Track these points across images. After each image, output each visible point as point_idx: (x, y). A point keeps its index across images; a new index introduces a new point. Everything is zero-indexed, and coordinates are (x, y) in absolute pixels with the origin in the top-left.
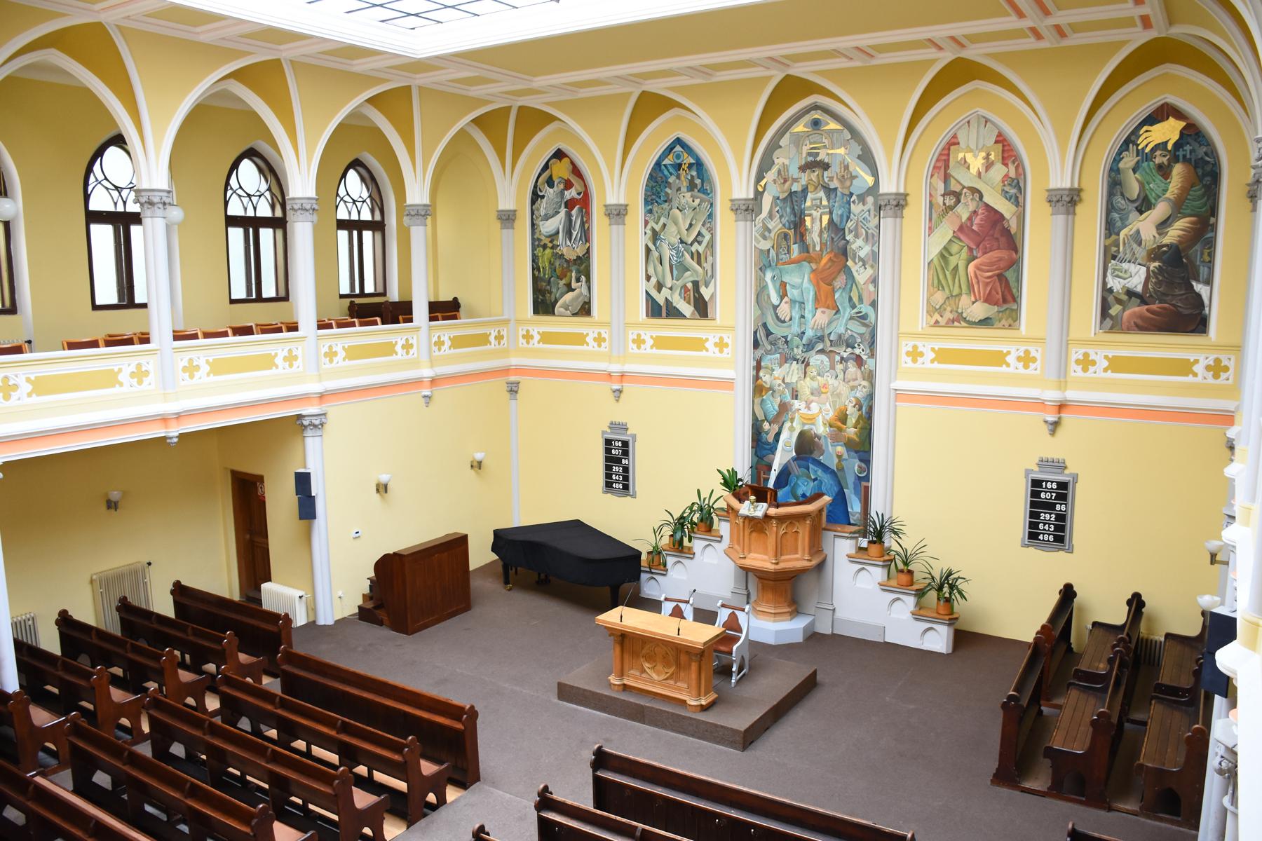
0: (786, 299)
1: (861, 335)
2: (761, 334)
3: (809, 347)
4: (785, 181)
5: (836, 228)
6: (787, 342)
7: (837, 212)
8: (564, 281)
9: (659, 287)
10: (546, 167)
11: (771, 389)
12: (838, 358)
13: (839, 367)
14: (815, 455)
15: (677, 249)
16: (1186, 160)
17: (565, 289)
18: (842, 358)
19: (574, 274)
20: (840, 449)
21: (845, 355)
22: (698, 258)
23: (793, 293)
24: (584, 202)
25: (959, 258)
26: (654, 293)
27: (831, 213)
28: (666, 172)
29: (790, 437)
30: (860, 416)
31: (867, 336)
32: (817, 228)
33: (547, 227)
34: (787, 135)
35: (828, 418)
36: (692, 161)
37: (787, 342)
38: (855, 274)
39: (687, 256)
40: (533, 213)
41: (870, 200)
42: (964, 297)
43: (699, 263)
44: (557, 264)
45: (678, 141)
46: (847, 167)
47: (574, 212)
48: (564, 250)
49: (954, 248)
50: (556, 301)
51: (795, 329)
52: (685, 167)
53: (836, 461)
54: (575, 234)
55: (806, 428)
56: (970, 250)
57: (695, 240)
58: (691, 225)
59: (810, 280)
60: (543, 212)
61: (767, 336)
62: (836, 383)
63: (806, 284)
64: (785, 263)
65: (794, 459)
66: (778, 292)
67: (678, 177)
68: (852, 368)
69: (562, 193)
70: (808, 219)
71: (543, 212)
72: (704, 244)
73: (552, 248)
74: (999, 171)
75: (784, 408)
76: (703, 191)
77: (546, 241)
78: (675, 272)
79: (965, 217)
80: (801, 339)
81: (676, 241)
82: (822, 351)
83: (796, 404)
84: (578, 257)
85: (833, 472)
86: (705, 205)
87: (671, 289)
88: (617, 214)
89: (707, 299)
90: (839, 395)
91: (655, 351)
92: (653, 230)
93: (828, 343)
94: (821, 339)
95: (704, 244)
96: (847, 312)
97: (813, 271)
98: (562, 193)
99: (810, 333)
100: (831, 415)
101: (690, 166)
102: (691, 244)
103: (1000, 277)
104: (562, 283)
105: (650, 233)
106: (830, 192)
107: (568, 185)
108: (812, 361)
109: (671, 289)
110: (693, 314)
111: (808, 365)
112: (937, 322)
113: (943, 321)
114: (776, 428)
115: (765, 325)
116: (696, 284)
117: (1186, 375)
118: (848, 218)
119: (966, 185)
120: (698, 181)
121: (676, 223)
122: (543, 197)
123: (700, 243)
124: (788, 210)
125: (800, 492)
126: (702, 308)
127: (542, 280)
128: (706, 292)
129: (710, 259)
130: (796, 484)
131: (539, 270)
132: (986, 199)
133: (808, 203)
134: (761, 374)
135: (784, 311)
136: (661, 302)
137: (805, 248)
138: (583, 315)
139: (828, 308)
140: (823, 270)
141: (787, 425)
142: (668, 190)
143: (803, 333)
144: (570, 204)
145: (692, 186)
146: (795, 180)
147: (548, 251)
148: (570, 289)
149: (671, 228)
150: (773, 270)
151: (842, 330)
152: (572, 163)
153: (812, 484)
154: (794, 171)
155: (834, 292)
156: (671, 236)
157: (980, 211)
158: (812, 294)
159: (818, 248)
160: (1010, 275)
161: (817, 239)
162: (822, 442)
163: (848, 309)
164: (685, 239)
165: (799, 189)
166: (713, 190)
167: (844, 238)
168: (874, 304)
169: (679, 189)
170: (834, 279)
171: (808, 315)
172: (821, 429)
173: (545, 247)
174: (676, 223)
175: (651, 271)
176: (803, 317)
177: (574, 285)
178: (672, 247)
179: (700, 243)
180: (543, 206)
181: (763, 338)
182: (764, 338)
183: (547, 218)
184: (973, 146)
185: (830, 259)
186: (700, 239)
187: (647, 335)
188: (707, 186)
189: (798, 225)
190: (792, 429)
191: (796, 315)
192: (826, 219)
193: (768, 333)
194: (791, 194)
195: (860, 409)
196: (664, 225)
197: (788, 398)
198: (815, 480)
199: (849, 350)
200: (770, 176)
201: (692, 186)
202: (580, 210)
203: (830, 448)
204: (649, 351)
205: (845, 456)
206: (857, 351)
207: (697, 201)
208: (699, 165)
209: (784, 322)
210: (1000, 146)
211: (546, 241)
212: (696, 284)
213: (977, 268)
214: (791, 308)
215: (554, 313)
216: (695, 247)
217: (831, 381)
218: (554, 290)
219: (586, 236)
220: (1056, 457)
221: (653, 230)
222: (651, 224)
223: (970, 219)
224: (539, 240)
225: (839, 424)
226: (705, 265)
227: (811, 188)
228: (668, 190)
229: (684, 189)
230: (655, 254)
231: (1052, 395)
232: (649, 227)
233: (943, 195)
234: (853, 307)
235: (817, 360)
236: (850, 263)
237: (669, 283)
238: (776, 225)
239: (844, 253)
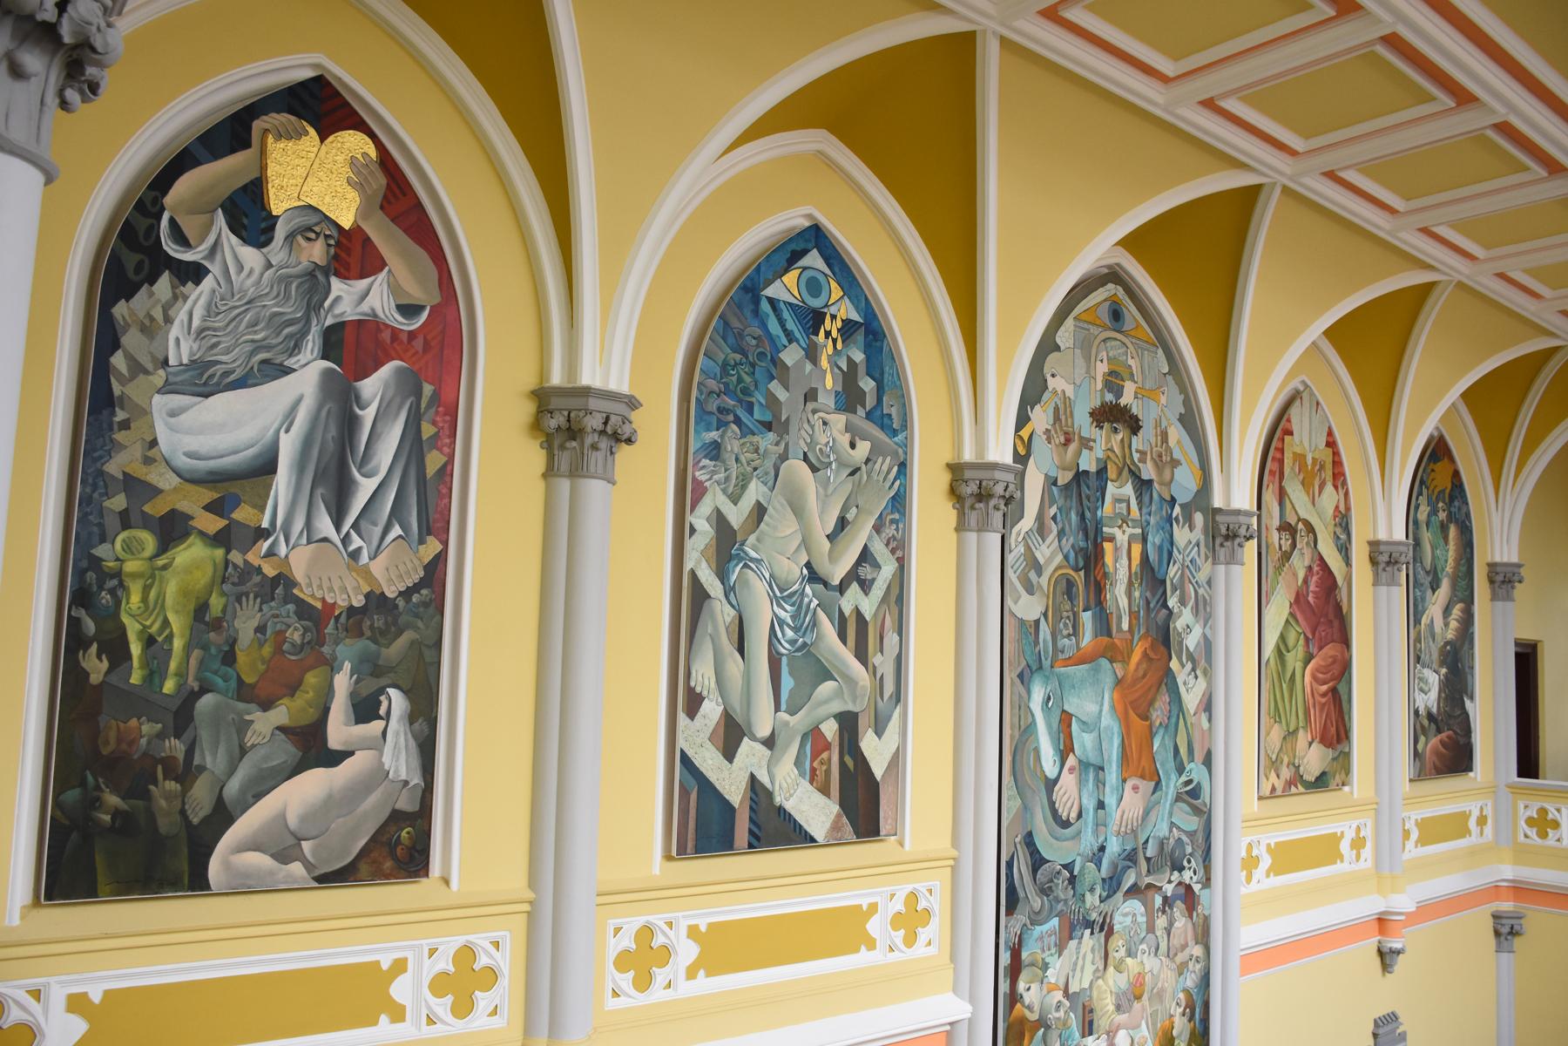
0: (1071, 761)
1: (1191, 834)
2: (1022, 866)
3: (1112, 884)
4: (1068, 441)
5: (1151, 577)
6: (1072, 880)
7: (1155, 539)
8: (280, 715)
9: (731, 735)
10: (233, 131)
11: (1042, 1023)
12: (1158, 901)
15: (796, 599)
16: (1457, 522)
17: (287, 752)
19: (342, 682)
22: (858, 633)
23: (1084, 741)
24: (435, 349)
25: (1294, 659)
26: (709, 761)
27: (1144, 540)
28: (774, 326)
30: (1192, 1034)
31: (1200, 837)
32: (1122, 575)
33: (199, 431)
34: (1069, 322)
36: (855, 316)
37: (1072, 880)
38: (1182, 689)
39: (828, 629)
40: (103, 337)
41: (1199, 518)
42: (1301, 732)
43: (862, 655)
44: (245, 624)
45: (815, 236)
46: (1164, 436)
47: (373, 386)
48: (300, 562)
49: (1292, 637)
50: (223, 816)
51: (1088, 842)
52: (834, 327)
54: (366, 487)
56: (1307, 640)
57: (853, 576)
58: (842, 523)
59: (1113, 707)
60: (180, 346)
61: (1035, 871)
63: (1109, 721)
64: (1070, 662)
66: (1055, 742)
67: (812, 354)
69: (313, 285)
70: (1107, 546)
71: (180, 346)
72: (878, 591)
73: (221, 540)
74: (1329, 498)
76: (878, 417)
77: (192, 503)
78: (787, 682)
79: (1301, 574)
80: (1099, 865)
81: (793, 570)
82: (1134, 891)
84: (377, 601)
86: (884, 464)
87: (769, 743)
88: (574, 430)
89: (878, 771)
91: (705, 984)
92: (720, 521)
93: (1144, 865)
94: (1131, 857)
95: (878, 591)
96: (1173, 784)
97: (1119, 682)
98: (313, 285)
99: (1114, 847)
101: (848, 328)
102: (842, 588)
103: (1334, 690)
104: (264, 723)
105: (700, 520)
106: (1143, 486)
107: (352, 254)
108: (1120, 922)
109: (769, 743)
110: (836, 827)
111: (1110, 933)
112: (1274, 789)
113: (1279, 785)
115: (1029, 840)
116: (849, 723)
117: (1463, 836)
118: (1170, 554)
119: (1303, 515)
120: (867, 385)
121: (798, 510)
122: (195, 273)
123: (866, 586)
124: (1073, 516)
126: (863, 806)
127: (142, 702)
128: (877, 751)
129: (892, 639)
131: (116, 650)
132: (1320, 546)
133: (1108, 508)
134: (1021, 986)
135: (1068, 792)
136: (735, 793)
137: (1104, 624)
138: (379, 875)
139: (1143, 777)
140: (1135, 681)
142: (775, 386)
143: (1102, 849)
144: (352, 348)
145: (849, 398)
146: (1086, 443)
147: (192, 556)
148: (312, 748)
149: (782, 525)
150: (1047, 679)
151: (1162, 830)
152: (386, 162)
154: (1082, 421)
155: (1152, 736)
156: (780, 551)
157: (1316, 569)
158: (1116, 742)
159: (1125, 626)
160: (1342, 688)
161: (1123, 602)
163: (1173, 777)
164: (823, 568)
165: (1093, 468)
166: (906, 424)
167: (1165, 605)
168: (1208, 761)
169: (811, 396)
170: (1151, 704)
171: (1110, 800)
173: (172, 530)
174: (798, 510)
175: (703, 675)
176: (1101, 805)
177: (339, 731)
178: (781, 592)
179: (866, 586)
180: (182, 323)
181: (1032, 886)
182: (1027, 878)
183: (203, 381)
184: (1306, 444)
185: (1145, 654)
186: (866, 572)
187: (678, 927)
188: (891, 408)
189: (1090, 558)
191: (1089, 804)
192: (1137, 550)
193: (1037, 861)
194: (1080, 476)
195: (1191, 1019)
196: (760, 511)
199: (1175, 876)
200: (1040, 418)
201: (849, 398)
202: (409, 385)
204: (686, 988)
206: (1187, 876)
207: (864, 447)
208: (869, 330)
209: (1066, 824)
210: (1330, 451)
211: (192, 503)
212: (849, 723)
213: (1314, 677)
214: (1081, 783)
215: (198, 882)
216: (852, 599)
218: (212, 759)
219: (429, 500)
220: (1385, 1012)
221: (720, 521)
222: (715, 499)
223: (1305, 581)
224: (133, 485)
226: (877, 659)
227: (1112, 472)
228: (775, 386)
229: (826, 400)
230: (722, 612)
231: (1368, 905)
232: (706, 508)
233: (1278, 530)
234: (1180, 770)
235: (1127, 913)
236: (1174, 664)
237: (764, 720)
238: (1049, 553)
239: (1164, 639)
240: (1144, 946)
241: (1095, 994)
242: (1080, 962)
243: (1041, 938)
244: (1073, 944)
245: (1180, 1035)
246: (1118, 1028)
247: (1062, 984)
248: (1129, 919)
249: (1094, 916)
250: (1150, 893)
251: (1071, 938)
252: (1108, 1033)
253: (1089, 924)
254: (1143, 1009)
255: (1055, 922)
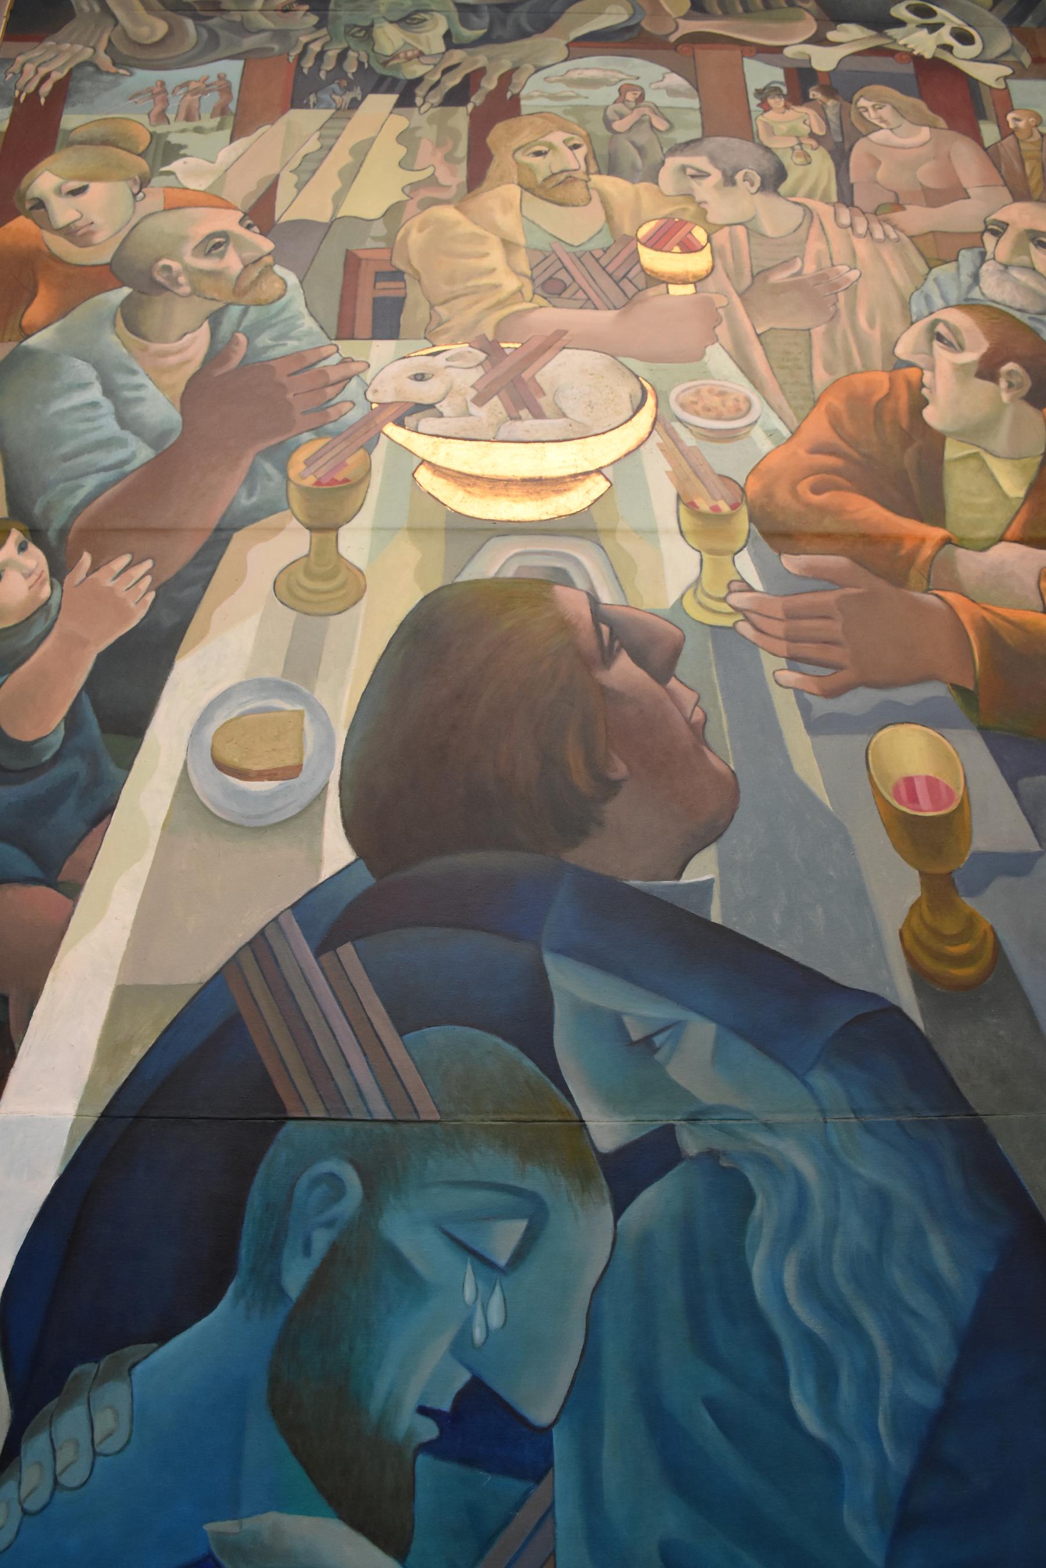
13: (785, 126)
14: (622, 848)
18: (801, 82)
20: (911, 751)
21: (824, 59)
29: (302, 665)
35: (734, 462)
53: (895, 888)
55: (492, 563)
62: (776, 216)
65: (332, 920)
68: (899, 136)
75: (246, 405)
83: (385, 366)
85: (874, 1027)
90: (823, 293)
100: (764, 437)
114: (127, 589)
125: (413, 1377)
130: (359, 1264)
141: (269, 552)
153: (589, 1234)
162: (698, 685)
172: (669, 574)
190: (319, 589)
197: (296, 317)
198: (626, 1174)
203: (803, 754)
205: (998, 824)
217: (729, 205)
225: (870, 513)
240: (701, 162)
241: (415, 237)
242: (340, 156)
243: (160, 92)
244: (306, 121)
245: (976, 432)
246: (554, 342)
247: (243, 190)
248: (613, 93)
249: (416, 70)
250: (710, 57)
251: (297, 100)
252: (491, 349)
253: (407, 96)
254: (711, 317)
255: (233, 70)
